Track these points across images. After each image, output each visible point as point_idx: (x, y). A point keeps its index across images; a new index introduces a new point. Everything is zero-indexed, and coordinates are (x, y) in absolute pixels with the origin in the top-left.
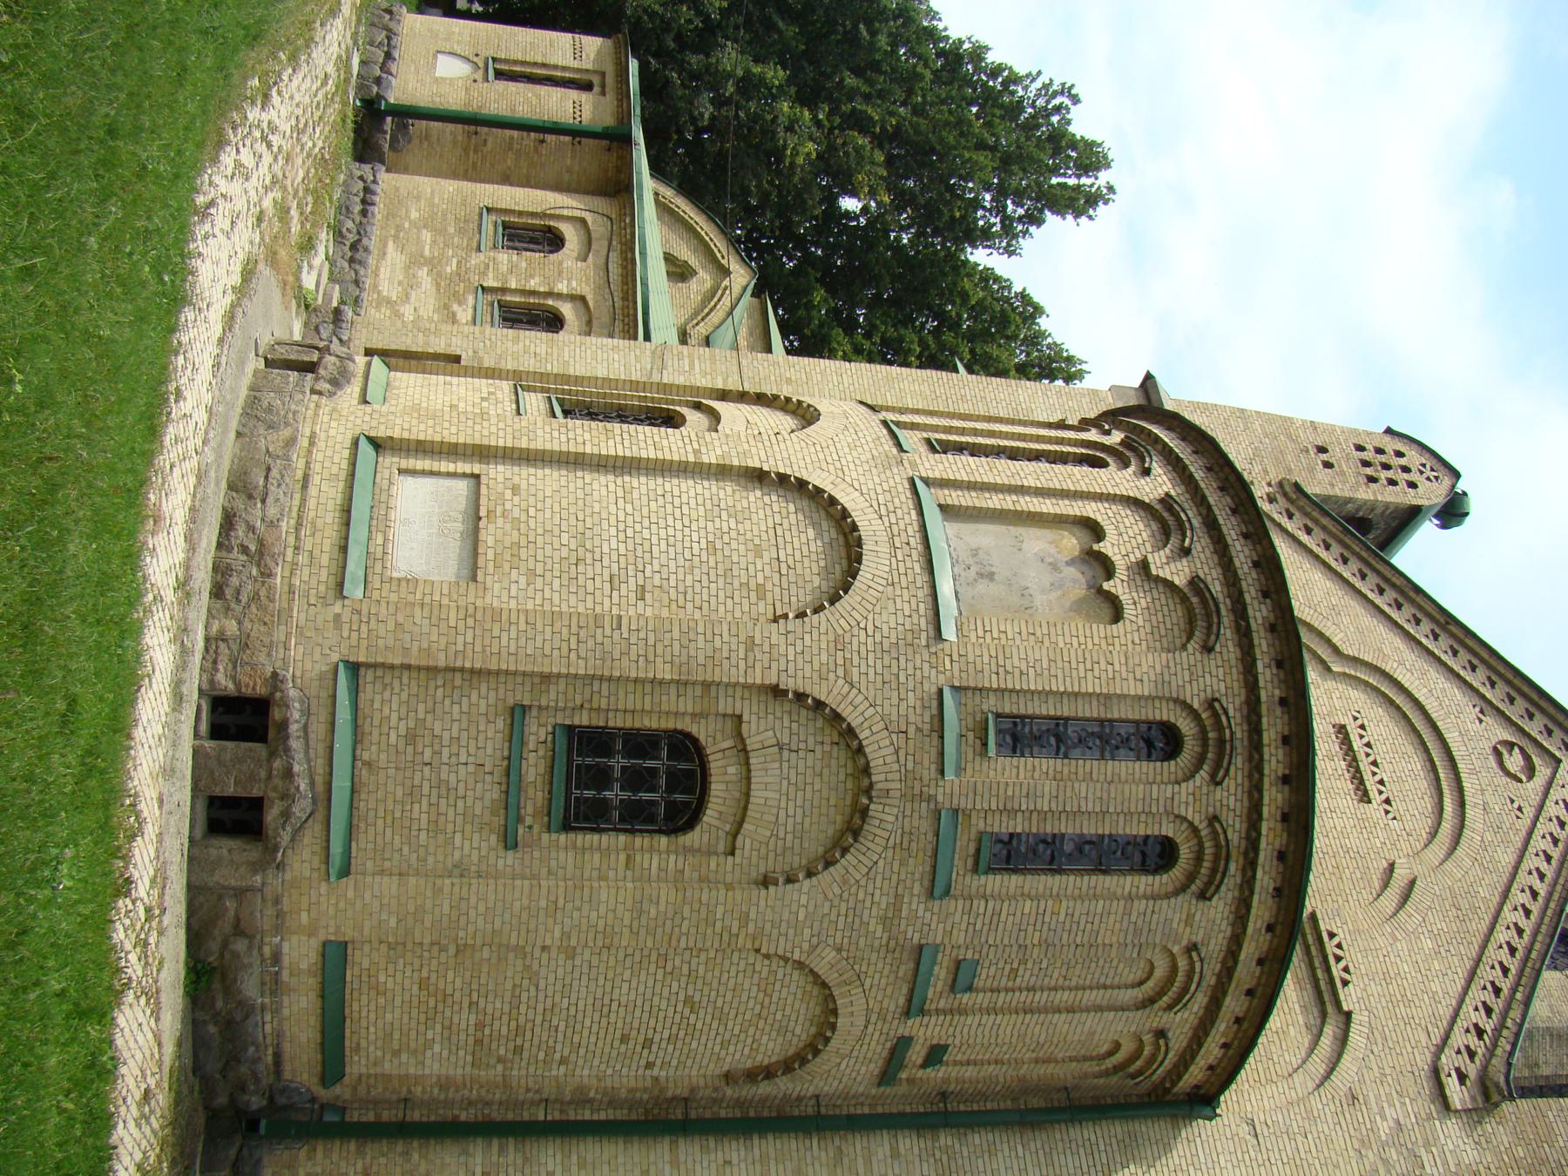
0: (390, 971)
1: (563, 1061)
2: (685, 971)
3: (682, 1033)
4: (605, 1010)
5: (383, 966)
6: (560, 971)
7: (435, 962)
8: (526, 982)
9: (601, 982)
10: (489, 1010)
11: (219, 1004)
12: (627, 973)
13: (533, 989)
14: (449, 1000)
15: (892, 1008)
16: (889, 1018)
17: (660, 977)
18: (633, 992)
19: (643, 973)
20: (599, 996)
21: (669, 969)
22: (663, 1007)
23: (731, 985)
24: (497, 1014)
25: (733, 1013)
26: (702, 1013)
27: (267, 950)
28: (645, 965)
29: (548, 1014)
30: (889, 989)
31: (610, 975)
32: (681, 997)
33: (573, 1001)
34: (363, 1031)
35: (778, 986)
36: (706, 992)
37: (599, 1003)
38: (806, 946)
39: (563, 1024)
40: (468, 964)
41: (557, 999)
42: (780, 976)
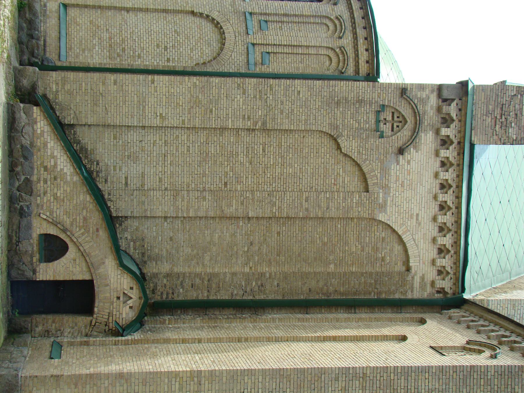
0: (81, 18)
1: (139, 57)
2: (173, 21)
3: (176, 44)
4: (150, 33)
5: (78, 16)
6: (134, 20)
7: (94, 16)
8: (123, 23)
9: (147, 24)
10: (113, 33)
11: (27, 15)
12: (155, 22)
13: (126, 25)
14: (100, 29)
15: (242, 31)
16: (242, 34)
17: (165, 23)
18: (157, 28)
19: (160, 21)
20: (147, 28)
21: (167, 20)
22: (168, 33)
23: (188, 26)
24: (115, 34)
25: (191, 36)
26: (181, 35)
27: (42, 3)
28: (160, 19)
29: (132, 34)
30: (239, 24)
31: (149, 22)
32: (173, 30)
33: (139, 30)
34: (73, 40)
35: (203, 28)
36: (181, 28)
37: (147, 31)
38: (208, 10)
39: (137, 39)
40: (105, 16)
41: (134, 29)
42: (203, 24)
